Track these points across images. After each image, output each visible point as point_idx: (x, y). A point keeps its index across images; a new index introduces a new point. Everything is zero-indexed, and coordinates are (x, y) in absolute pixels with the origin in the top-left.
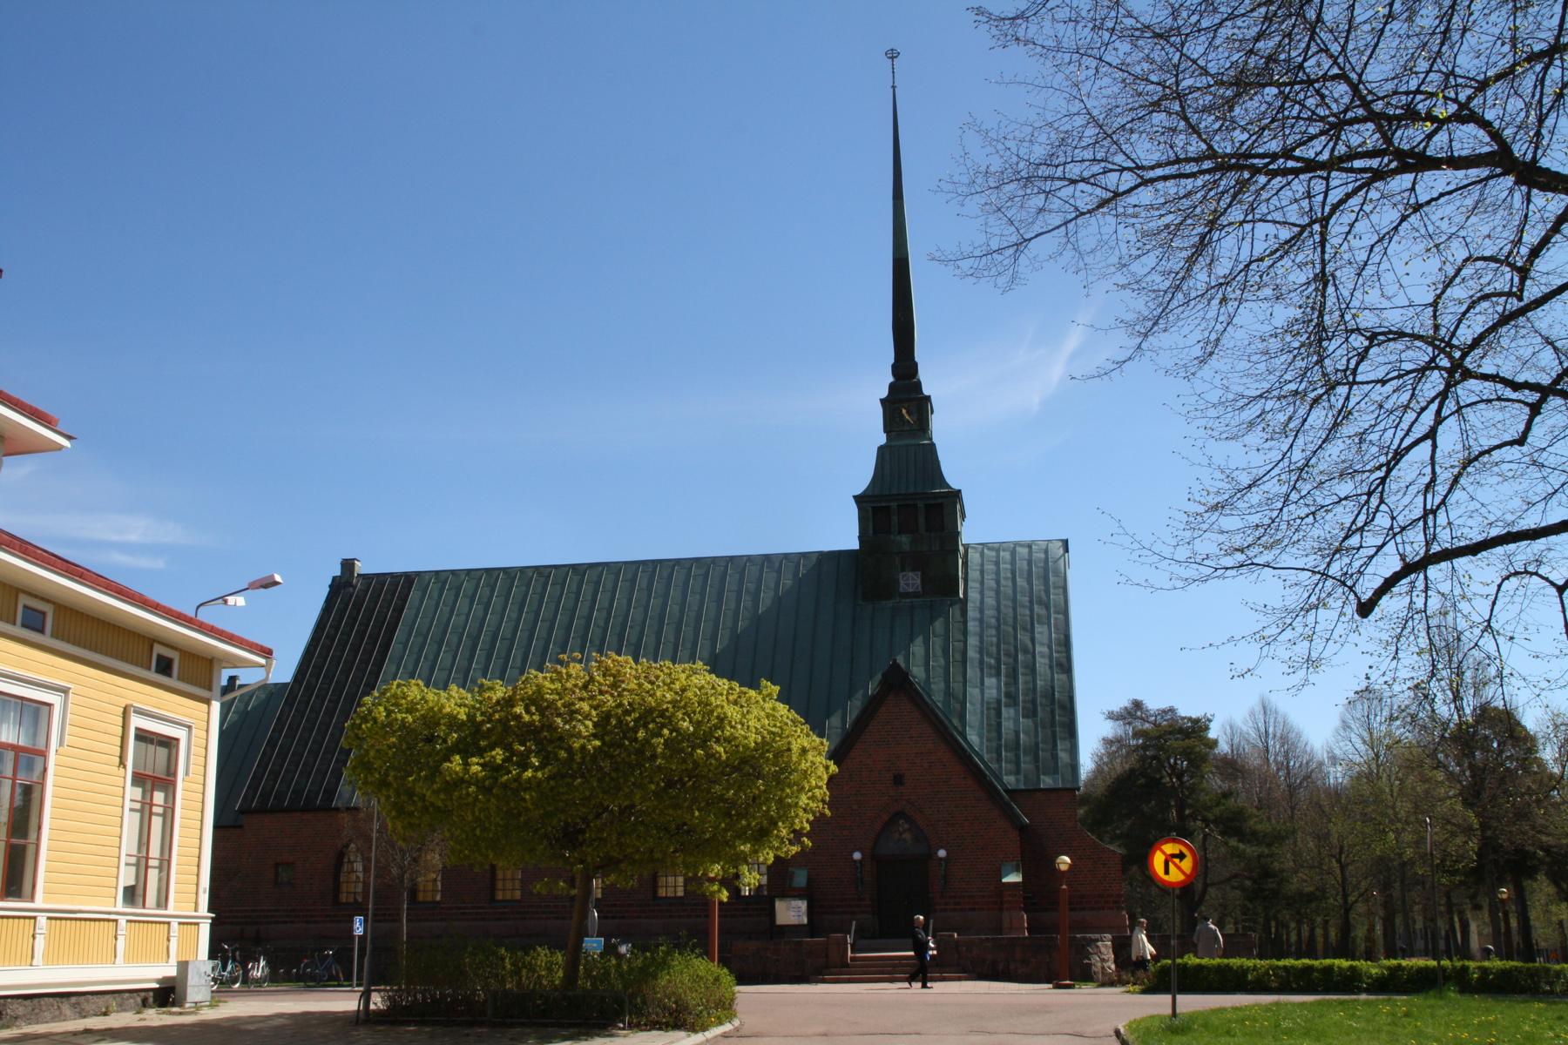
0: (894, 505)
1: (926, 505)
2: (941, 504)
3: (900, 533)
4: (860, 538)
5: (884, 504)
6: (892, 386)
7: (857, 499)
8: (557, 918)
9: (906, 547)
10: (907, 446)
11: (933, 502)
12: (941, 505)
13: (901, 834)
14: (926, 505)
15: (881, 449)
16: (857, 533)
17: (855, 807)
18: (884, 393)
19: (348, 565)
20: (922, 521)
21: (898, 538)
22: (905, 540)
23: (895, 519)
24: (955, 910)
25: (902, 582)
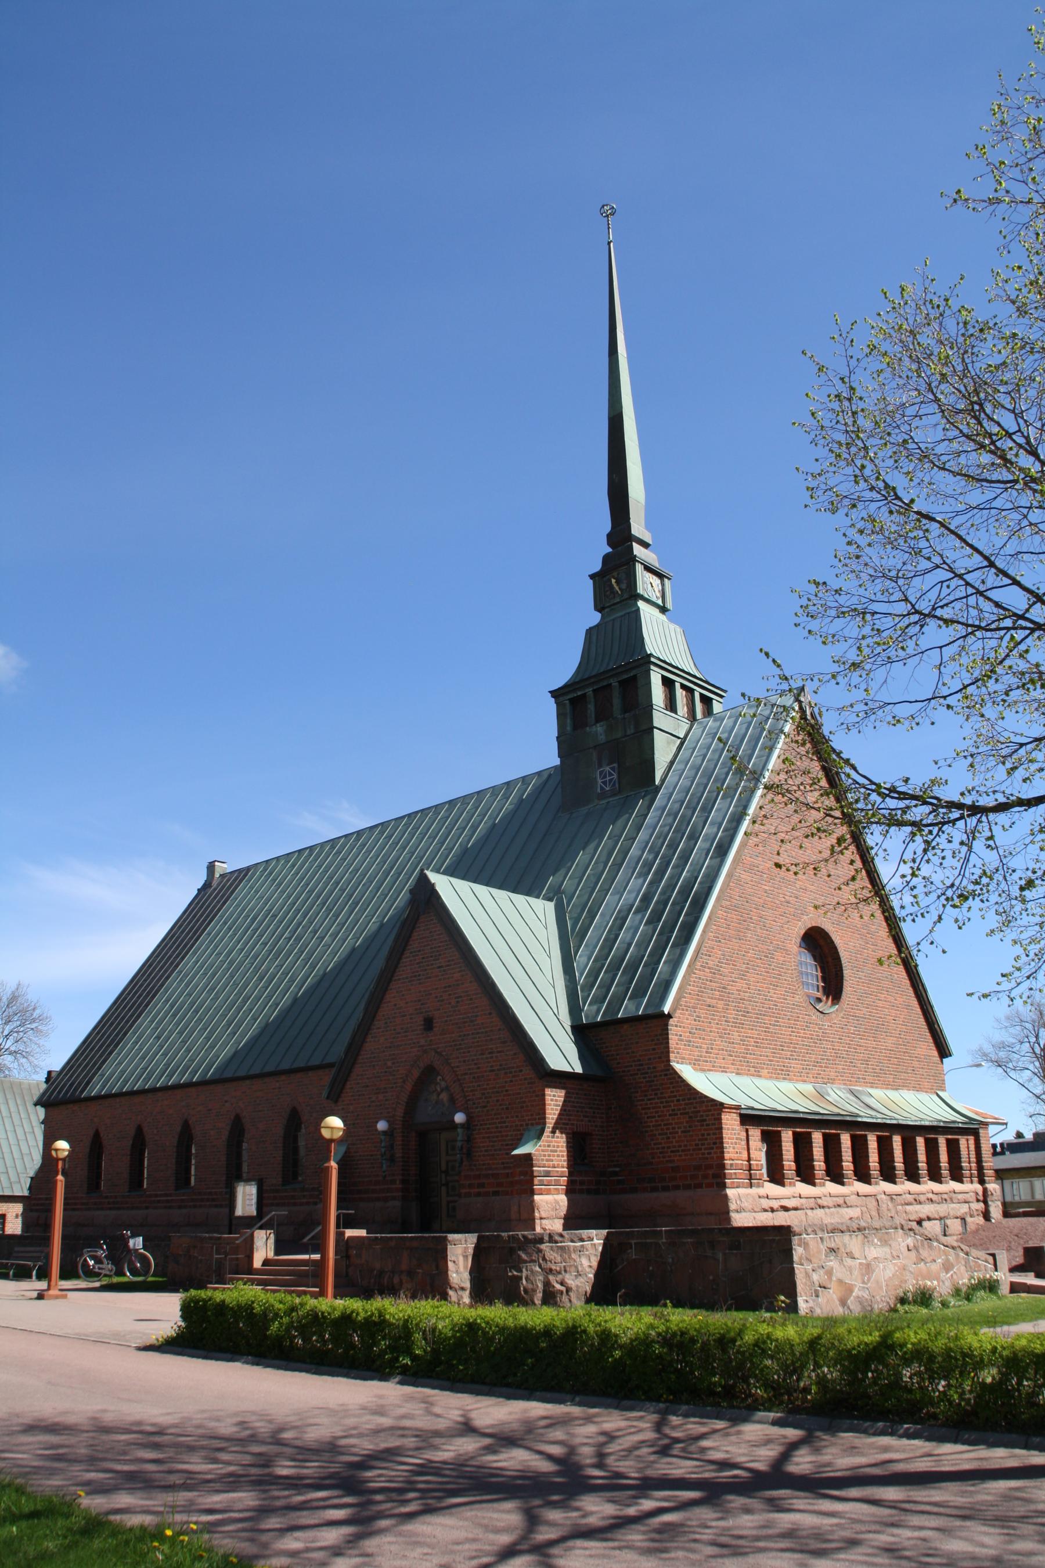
0: (589, 691)
1: (619, 682)
2: (635, 677)
3: (597, 721)
4: (562, 740)
5: (579, 693)
6: (606, 558)
7: (555, 694)
8: (216, 1206)
9: (602, 739)
10: (614, 620)
11: (625, 676)
12: (634, 678)
13: (439, 1095)
14: (619, 682)
15: (589, 632)
16: (554, 732)
17: (389, 1063)
18: (597, 567)
19: (211, 867)
20: (617, 702)
21: (594, 729)
22: (599, 729)
23: (591, 707)
24: (479, 1194)
25: (600, 781)
